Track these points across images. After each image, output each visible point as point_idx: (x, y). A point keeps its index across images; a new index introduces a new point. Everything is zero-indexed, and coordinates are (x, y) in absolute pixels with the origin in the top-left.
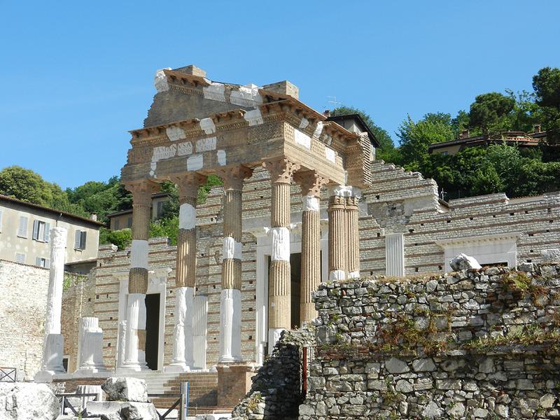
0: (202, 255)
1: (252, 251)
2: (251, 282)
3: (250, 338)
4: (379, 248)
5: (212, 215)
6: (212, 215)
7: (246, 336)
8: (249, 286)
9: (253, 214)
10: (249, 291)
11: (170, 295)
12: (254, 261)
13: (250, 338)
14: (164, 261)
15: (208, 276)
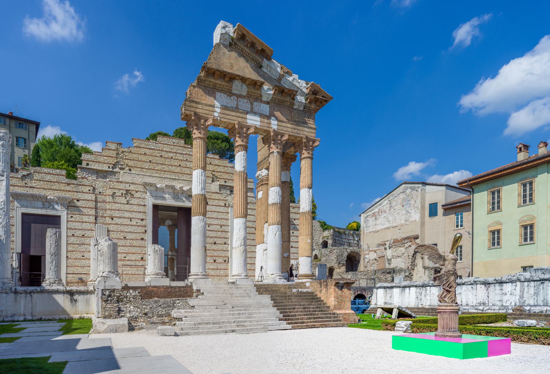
0: (100, 193)
1: (144, 199)
2: (142, 220)
3: (142, 258)
4: (226, 213)
5: (109, 164)
6: (109, 164)
7: (139, 257)
8: (140, 223)
9: (143, 171)
10: (142, 226)
11: (70, 220)
12: (144, 205)
13: (142, 258)
14: (64, 191)
15: (106, 210)
